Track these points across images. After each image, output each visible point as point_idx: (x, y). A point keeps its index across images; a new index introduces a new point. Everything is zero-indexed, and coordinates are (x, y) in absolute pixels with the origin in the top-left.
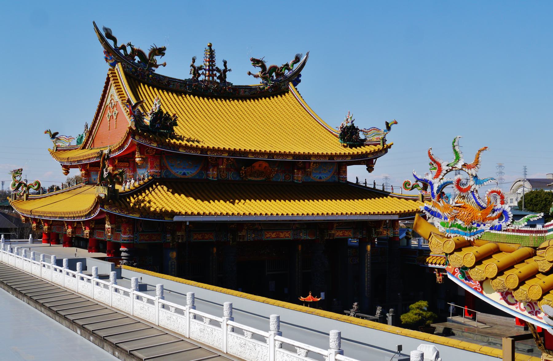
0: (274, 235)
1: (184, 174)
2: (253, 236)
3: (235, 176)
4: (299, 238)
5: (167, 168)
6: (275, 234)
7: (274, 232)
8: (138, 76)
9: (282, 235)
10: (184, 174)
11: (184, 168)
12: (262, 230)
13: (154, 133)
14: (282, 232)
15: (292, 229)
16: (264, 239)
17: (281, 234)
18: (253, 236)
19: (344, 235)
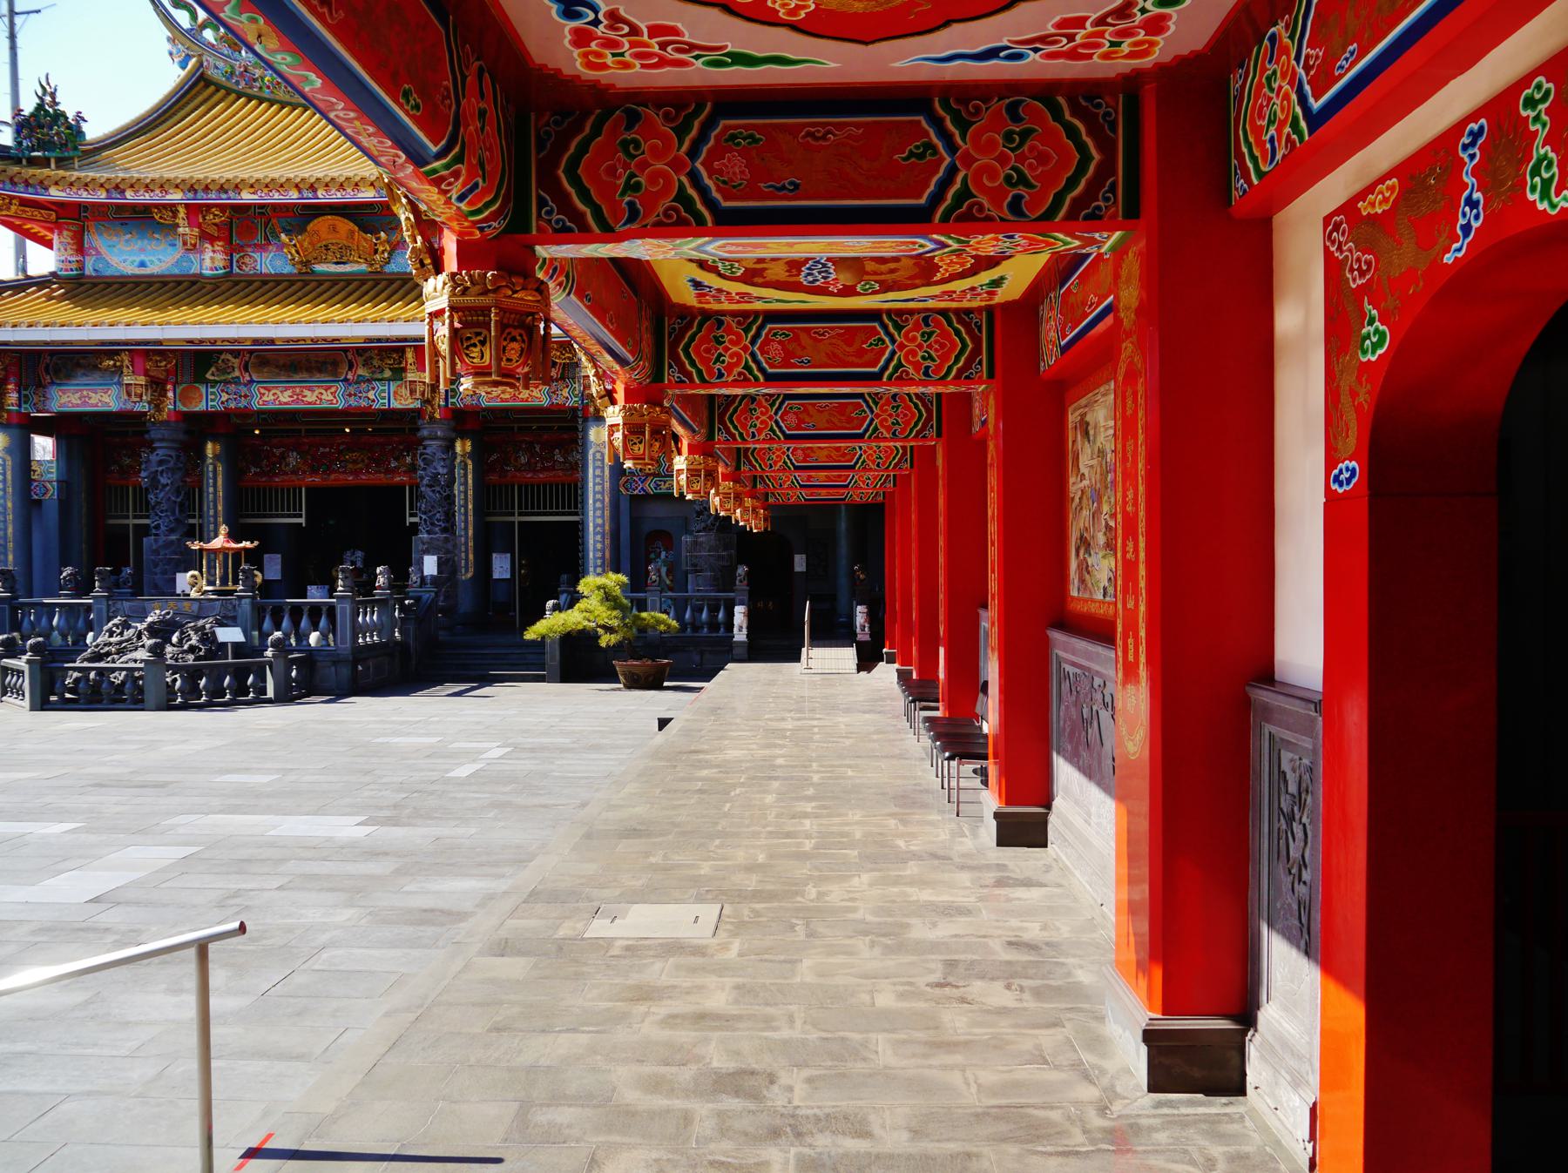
0: (285, 397)
1: (142, 264)
2: (225, 397)
3: (278, 263)
4: (364, 403)
5: (98, 253)
6: (289, 393)
7: (287, 389)
8: (237, 83)
9: (310, 397)
10: (142, 264)
11: (142, 250)
12: (252, 381)
13: (18, 161)
14: (310, 389)
15: (346, 380)
16: (256, 404)
17: (307, 392)
18: (225, 397)
19: (514, 398)
